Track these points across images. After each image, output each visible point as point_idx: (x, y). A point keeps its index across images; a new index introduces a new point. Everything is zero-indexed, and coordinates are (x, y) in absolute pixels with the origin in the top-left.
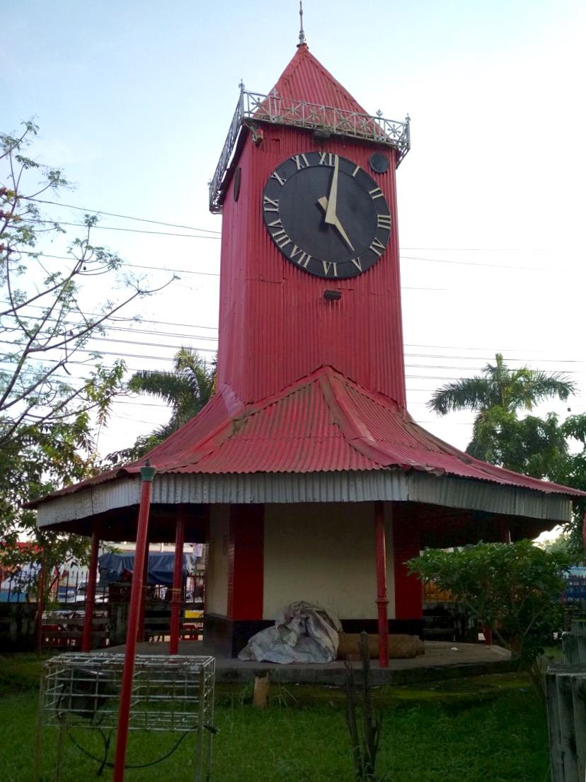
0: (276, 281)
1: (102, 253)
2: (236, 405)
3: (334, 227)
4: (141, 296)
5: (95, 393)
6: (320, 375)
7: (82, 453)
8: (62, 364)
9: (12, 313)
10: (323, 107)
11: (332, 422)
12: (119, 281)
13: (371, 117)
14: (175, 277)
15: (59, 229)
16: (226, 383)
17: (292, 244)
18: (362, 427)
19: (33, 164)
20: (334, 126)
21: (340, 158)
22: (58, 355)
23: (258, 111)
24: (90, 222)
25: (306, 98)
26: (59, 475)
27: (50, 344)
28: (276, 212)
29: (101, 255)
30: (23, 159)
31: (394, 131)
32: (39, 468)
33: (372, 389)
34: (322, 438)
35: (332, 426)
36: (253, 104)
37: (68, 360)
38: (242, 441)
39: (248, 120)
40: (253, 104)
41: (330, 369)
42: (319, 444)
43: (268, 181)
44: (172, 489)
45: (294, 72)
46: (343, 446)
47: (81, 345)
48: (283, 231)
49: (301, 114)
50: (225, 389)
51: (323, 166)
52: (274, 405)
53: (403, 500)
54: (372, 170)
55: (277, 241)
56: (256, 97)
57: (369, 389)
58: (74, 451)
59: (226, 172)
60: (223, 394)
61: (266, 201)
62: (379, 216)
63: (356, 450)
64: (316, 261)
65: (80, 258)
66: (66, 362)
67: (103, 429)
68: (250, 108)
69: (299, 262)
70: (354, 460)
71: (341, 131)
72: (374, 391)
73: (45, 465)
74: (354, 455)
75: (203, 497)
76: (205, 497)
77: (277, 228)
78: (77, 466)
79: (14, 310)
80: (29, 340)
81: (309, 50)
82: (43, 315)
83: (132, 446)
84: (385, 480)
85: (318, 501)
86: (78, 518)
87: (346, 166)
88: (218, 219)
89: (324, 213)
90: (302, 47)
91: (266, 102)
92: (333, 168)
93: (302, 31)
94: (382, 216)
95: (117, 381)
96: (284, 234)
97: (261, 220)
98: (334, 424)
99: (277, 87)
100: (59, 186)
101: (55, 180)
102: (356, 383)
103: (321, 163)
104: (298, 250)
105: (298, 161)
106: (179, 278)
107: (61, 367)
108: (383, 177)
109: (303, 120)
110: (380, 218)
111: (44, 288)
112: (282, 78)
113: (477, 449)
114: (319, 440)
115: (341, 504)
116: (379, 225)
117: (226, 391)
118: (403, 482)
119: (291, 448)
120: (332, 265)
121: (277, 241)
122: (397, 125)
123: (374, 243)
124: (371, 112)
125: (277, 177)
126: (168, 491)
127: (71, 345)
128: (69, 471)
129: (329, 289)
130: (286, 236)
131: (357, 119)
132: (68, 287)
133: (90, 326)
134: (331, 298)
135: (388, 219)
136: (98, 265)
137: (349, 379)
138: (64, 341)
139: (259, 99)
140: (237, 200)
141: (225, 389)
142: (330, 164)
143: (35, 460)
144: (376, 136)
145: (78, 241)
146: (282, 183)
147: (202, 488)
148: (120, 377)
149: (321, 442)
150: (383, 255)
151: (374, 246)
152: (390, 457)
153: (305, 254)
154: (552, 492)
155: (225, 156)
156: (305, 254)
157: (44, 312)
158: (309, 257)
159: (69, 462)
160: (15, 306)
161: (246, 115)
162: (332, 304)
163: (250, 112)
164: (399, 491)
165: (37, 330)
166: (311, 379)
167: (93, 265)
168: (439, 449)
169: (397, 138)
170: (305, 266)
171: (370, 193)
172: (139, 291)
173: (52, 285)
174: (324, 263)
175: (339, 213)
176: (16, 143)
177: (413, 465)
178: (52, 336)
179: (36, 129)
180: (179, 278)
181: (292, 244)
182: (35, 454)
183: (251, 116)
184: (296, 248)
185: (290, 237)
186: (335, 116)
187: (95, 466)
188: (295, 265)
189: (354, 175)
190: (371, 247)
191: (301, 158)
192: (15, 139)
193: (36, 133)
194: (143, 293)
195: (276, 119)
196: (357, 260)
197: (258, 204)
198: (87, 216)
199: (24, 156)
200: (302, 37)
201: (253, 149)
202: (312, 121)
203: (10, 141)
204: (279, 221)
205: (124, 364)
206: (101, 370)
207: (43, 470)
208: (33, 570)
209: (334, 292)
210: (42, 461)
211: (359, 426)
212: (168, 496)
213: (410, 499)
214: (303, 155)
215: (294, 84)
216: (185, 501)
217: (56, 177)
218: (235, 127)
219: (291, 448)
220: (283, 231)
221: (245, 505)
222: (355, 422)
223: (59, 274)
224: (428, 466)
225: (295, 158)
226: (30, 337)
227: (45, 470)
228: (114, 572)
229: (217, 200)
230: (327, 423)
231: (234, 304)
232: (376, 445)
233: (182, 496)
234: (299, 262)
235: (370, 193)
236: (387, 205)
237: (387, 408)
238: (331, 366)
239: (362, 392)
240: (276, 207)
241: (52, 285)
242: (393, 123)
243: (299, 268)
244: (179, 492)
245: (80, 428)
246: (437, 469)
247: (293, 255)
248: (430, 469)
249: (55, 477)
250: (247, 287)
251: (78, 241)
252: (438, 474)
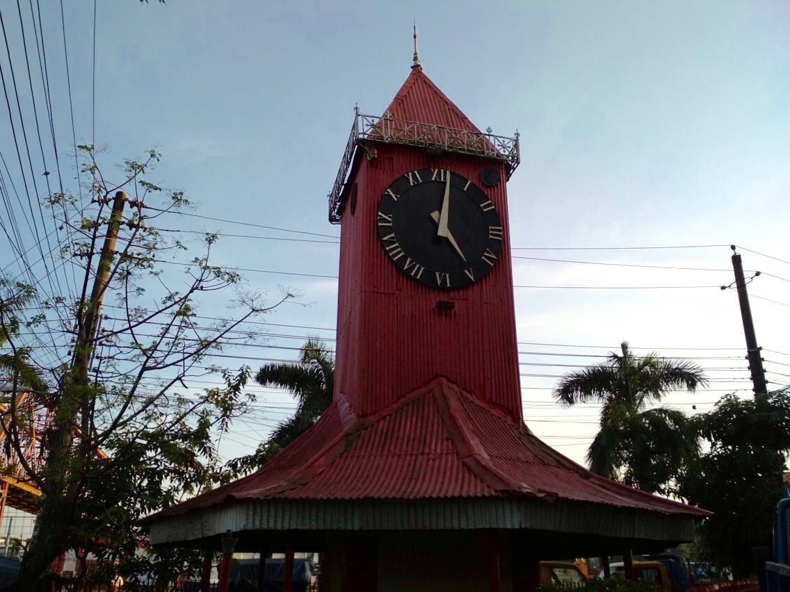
0: (390, 292)
1: (219, 272)
2: (350, 416)
3: (446, 239)
4: (256, 313)
5: (219, 399)
6: (433, 384)
7: (202, 460)
8: (179, 378)
9: (129, 331)
10: (435, 126)
11: (446, 435)
12: (233, 301)
13: (481, 134)
14: (289, 295)
15: (181, 247)
16: (341, 392)
17: (404, 259)
18: (474, 442)
19: (156, 189)
20: (446, 143)
21: (451, 172)
22: (172, 372)
23: (373, 132)
24: (211, 239)
25: (419, 118)
26: (179, 480)
27: (168, 361)
28: (390, 226)
29: (218, 273)
30: (147, 184)
31: (504, 147)
32: (160, 474)
33: (487, 399)
34: (435, 455)
35: (445, 442)
36: (367, 125)
37: (186, 374)
38: (355, 458)
39: (363, 141)
40: (367, 125)
41: (445, 381)
42: (431, 462)
43: (381, 198)
44: (280, 515)
45: (408, 92)
46: (456, 464)
47: (198, 360)
48: (397, 244)
49: (413, 132)
50: (341, 398)
51: (436, 181)
52: (388, 418)
53: (516, 527)
54: (483, 184)
55: (391, 254)
56: (370, 119)
57: (484, 399)
58: (195, 458)
59: (343, 187)
60: (339, 404)
61: (380, 216)
62: (490, 228)
63: (469, 470)
64: (429, 274)
65: (198, 277)
66: (184, 376)
67: (225, 435)
68: (365, 130)
69: (412, 274)
70: (466, 481)
71: (452, 148)
72: (490, 402)
73: (166, 471)
74: (467, 476)
75: (310, 523)
76: (313, 523)
77: (390, 242)
78: (197, 473)
79: (130, 328)
80: (145, 358)
81: (423, 71)
82: (162, 331)
83: (253, 453)
84: (496, 507)
85: (428, 528)
86: (188, 539)
87: (457, 181)
88: (337, 229)
89: (436, 226)
90: (416, 68)
91: (378, 123)
92: (445, 183)
93: (415, 54)
94: (493, 228)
95: (241, 387)
96: (397, 247)
97: (375, 233)
98: (447, 439)
99: (390, 109)
100: (181, 206)
101: (178, 200)
102: (470, 392)
103: (433, 179)
104: (411, 262)
105: (411, 178)
106: (292, 296)
107: (178, 382)
108: (494, 188)
109: (416, 138)
110: (492, 230)
111: (162, 307)
112: (396, 98)
113: (601, 450)
114: (431, 456)
115: (452, 530)
116: (491, 237)
117: (341, 402)
118: (515, 509)
119: (403, 466)
120: (445, 275)
121: (391, 254)
122: (507, 141)
123: (486, 254)
124: (483, 131)
125: (391, 193)
126: (276, 516)
127: (188, 362)
128: (190, 476)
129: (443, 300)
130: (399, 249)
132: (185, 312)
133: (205, 344)
134: (444, 309)
135: (500, 231)
136: (216, 282)
137: (463, 389)
138: (182, 358)
139: (373, 121)
140: (353, 213)
141: (341, 398)
142: (442, 180)
143: (155, 466)
144: (486, 152)
145: (197, 259)
146: (396, 199)
147: (310, 512)
148: (244, 384)
149: (434, 460)
150: (495, 265)
151: (486, 257)
152: (501, 480)
153: (418, 266)
154: (673, 513)
155: (342, 173)
156: (418, 266)
157: (162, 328)
158: (422, 268)
159: (189, 469)
160: (133, 324)
161: (361, 136)
162: (446, 316)
163: (364, 134)
164: (511, 519)
165: (155, 347)
166: (423, 391)
167: (210, 281)
168: (555, 463)
169: (507, 153)
170: (418, 277)
171: (482, 206)
172: (254, 310)
173: (169, 303)
174: (437, 274)
175: (451, 226)
176: (141, 168)
177: (524, 491)
178: (168, 355)
179: (159, 157)
180: (292, 296)
181: (404, 259)
182: (156, 461)
183: (366, 137)
184: (409, 260)
186: (446, 134)
187: (215, 471)
190: (483, 258)
191: (414, 176)
192: (139, 164)
193: (158, 160)
194: (257, 311)
195: (389, 139)
196: (469, 271)
197: (373, 220)
198: (207, 234)
199: (147, 182)
200: (415, 59)
201: (367, 167)
202: (424, 139)
203: (135, 166)
204: (393, 235)
205: (249, 370)
206: (227, 376)
207: (164, 476)
208: (150, 580)
209: (447, 303)
210: (162, 468)
211: (472, 442)
212: (276, 522)
213: (523, 526)
214: (416, 172)
215: (407, 104)
216: (293, 527)
217: (179, 197)
218: (351, 147)
219: (403, 466)
220: (397, 244)
221: (353, 531)
222: (469, 438)
223: (177, 293)
224: (541, 491)
225: (408, 175)
226: (147, 356)
227: (166, 477)
228: (232, 581)
229: (336, 210)
230: (440, 437)
231: (350, 314)
232: (490, 465)
233: (290, 522)
234: (412, 274)
235: (482, 206)
236: (499, 218)
237: (503, 419)
238: (446, 377)
239: (477, 402)
240: (388, 222)
241: (169, 303)
242: (503, 139)
243: (413, 279)
244: (287, 518)
245: (200, 436)
246: (549, 494)
247: (406, 267)
248: (542, 495)
249: (176, 483)
250: (361, 299)
251: (197, 259)
252: (550, 500)
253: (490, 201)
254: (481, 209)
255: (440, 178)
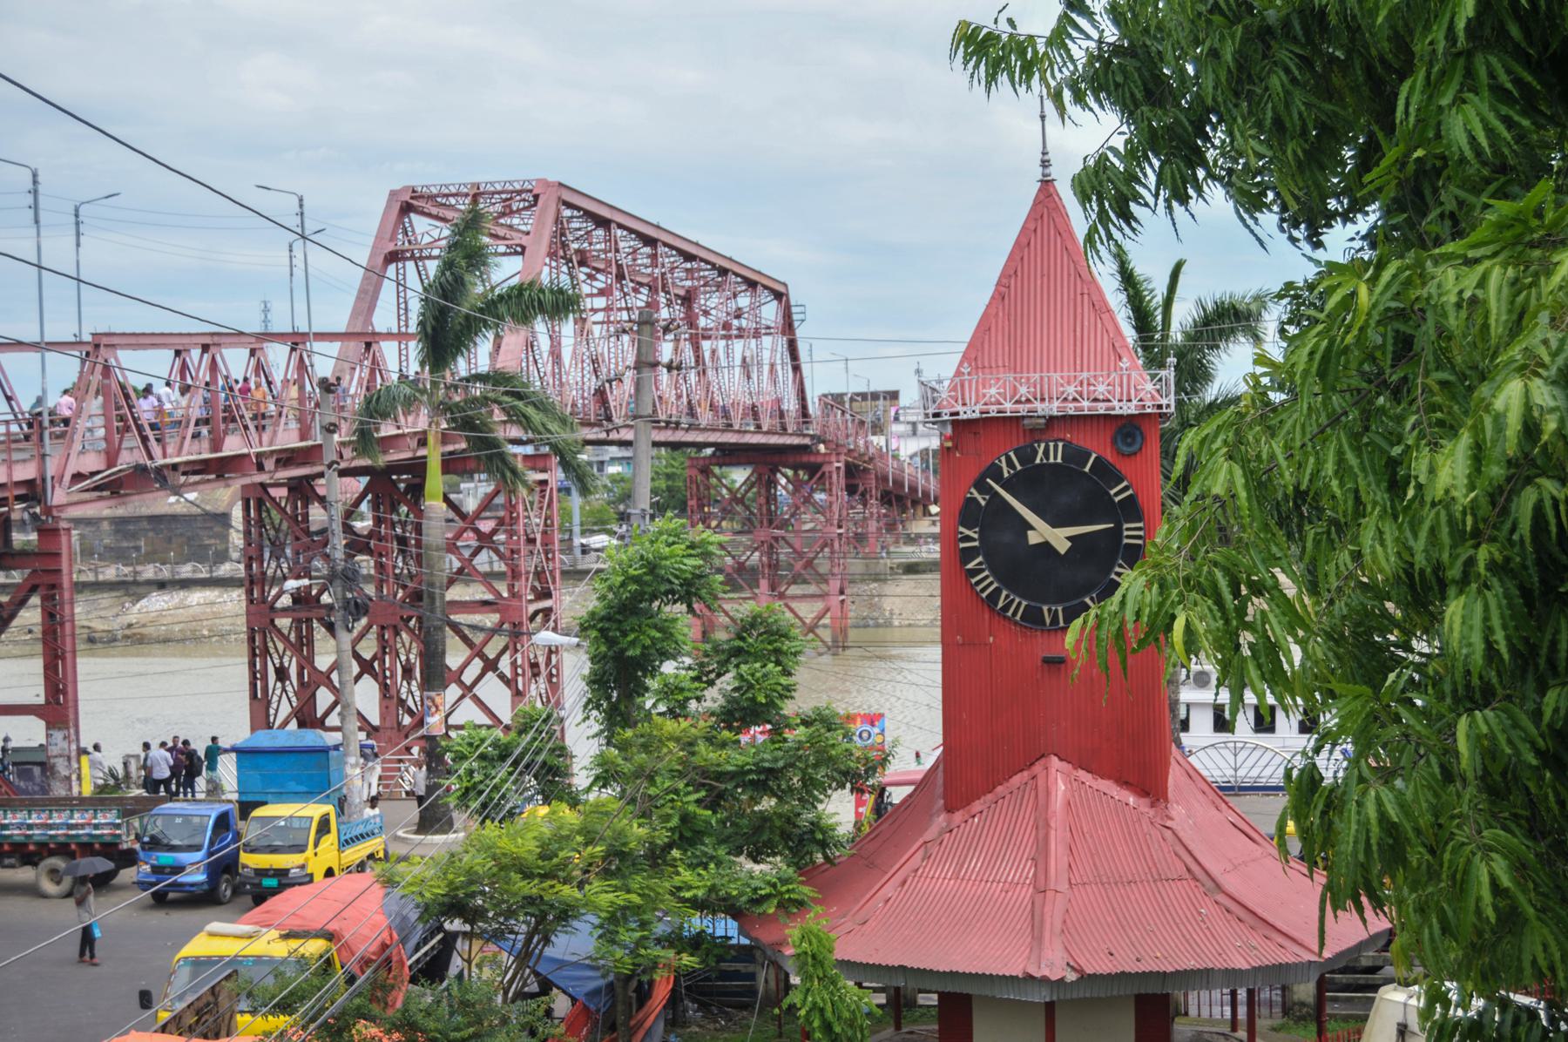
6: (1038, 768)
17: (997, 591)
48: (986, 573)
55: (979, 588)
96: (986, 577)
121: (979, 588)
131: (1081, 394)
171: (1112, 492)
181: (997, 591)
185: (998, 579)
188: (1005, 617)
189: (1087, 469)
191: (1009, 461)
204: (980, 559)
235: (1112, 492)
240: (974, 540)
253: (1125, 483)
254: (1111, 499)
255: (1048, 459)
